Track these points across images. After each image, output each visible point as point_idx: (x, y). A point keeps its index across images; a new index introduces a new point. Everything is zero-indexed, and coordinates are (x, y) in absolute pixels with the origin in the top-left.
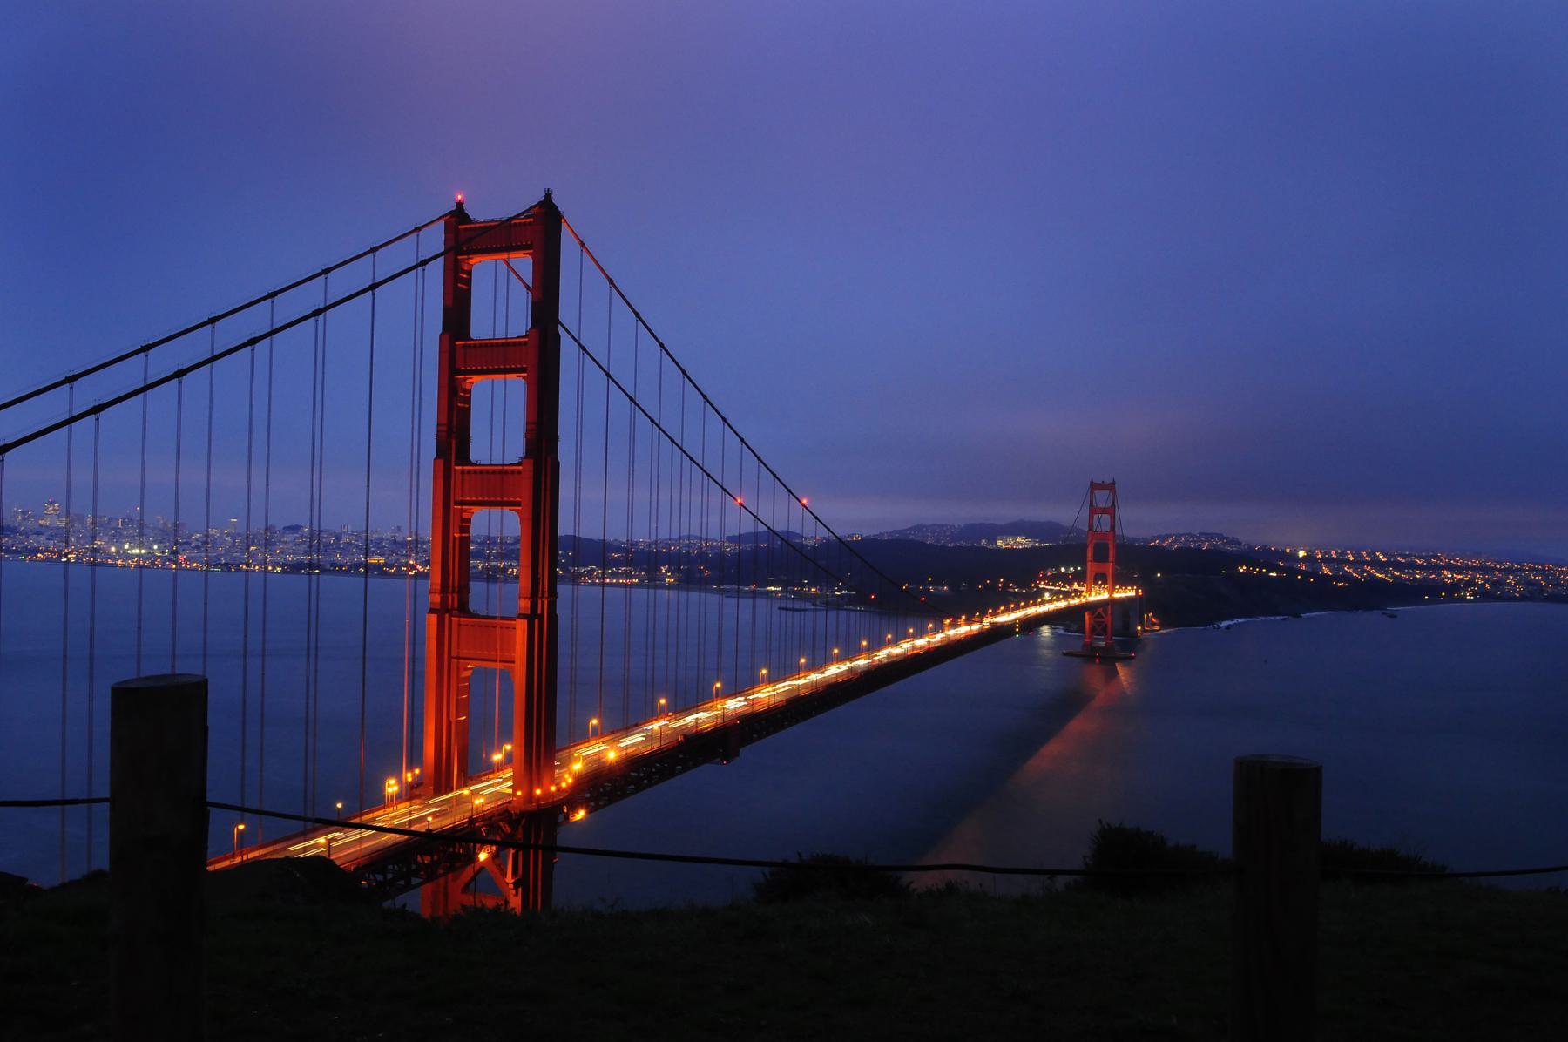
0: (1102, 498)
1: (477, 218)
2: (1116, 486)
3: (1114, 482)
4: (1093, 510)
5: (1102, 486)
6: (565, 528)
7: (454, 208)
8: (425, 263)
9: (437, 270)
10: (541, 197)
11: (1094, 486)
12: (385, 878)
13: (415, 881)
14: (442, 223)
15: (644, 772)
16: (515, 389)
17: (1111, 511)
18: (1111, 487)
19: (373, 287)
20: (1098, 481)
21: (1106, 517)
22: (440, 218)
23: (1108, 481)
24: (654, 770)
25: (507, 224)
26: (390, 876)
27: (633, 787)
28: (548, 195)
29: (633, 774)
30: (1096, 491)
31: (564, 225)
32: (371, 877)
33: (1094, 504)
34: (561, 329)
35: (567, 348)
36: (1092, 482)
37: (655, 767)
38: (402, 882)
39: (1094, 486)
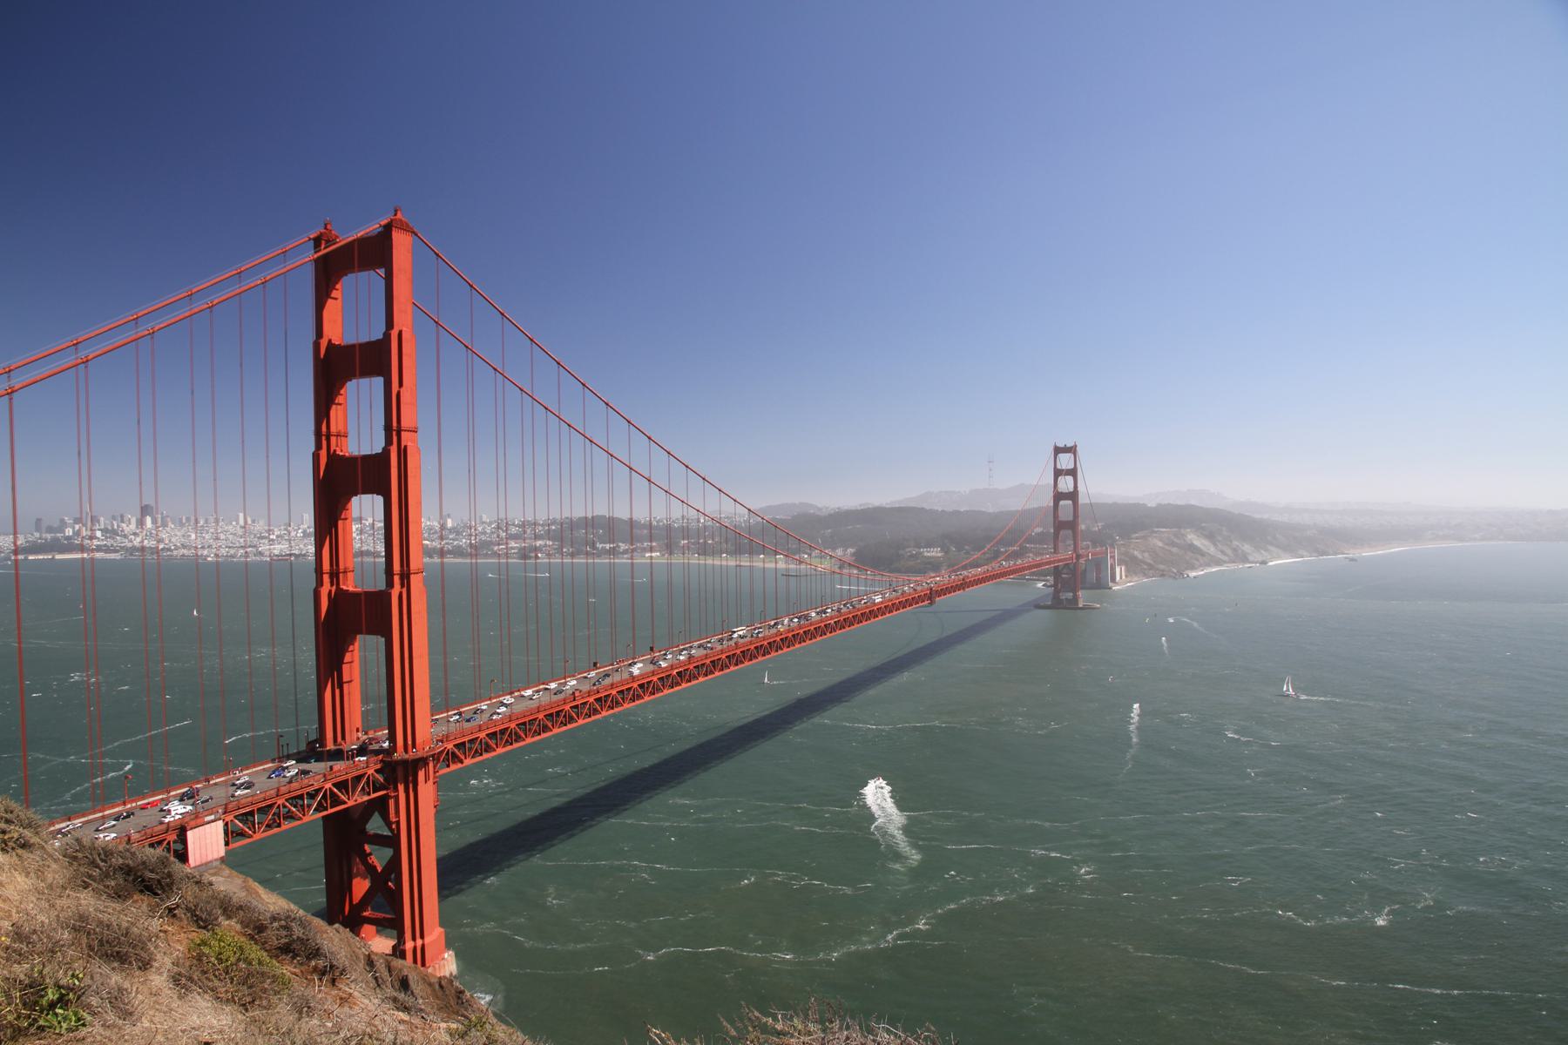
0: (1065, 461)
2: (1078, 448)
3: (1076, 446)
4: (1058, 473)
5: (1066, 450)
14: (312, 242)
17: (1073, 473)
18: (1072, 450)
20: (1063, 446)
21: (1070, 479)
22: (310, 239)
23: (1068, 445)
25: (362, 241)
30: (1060, 455)
33: (1059, 467)
39: (1058, 450)
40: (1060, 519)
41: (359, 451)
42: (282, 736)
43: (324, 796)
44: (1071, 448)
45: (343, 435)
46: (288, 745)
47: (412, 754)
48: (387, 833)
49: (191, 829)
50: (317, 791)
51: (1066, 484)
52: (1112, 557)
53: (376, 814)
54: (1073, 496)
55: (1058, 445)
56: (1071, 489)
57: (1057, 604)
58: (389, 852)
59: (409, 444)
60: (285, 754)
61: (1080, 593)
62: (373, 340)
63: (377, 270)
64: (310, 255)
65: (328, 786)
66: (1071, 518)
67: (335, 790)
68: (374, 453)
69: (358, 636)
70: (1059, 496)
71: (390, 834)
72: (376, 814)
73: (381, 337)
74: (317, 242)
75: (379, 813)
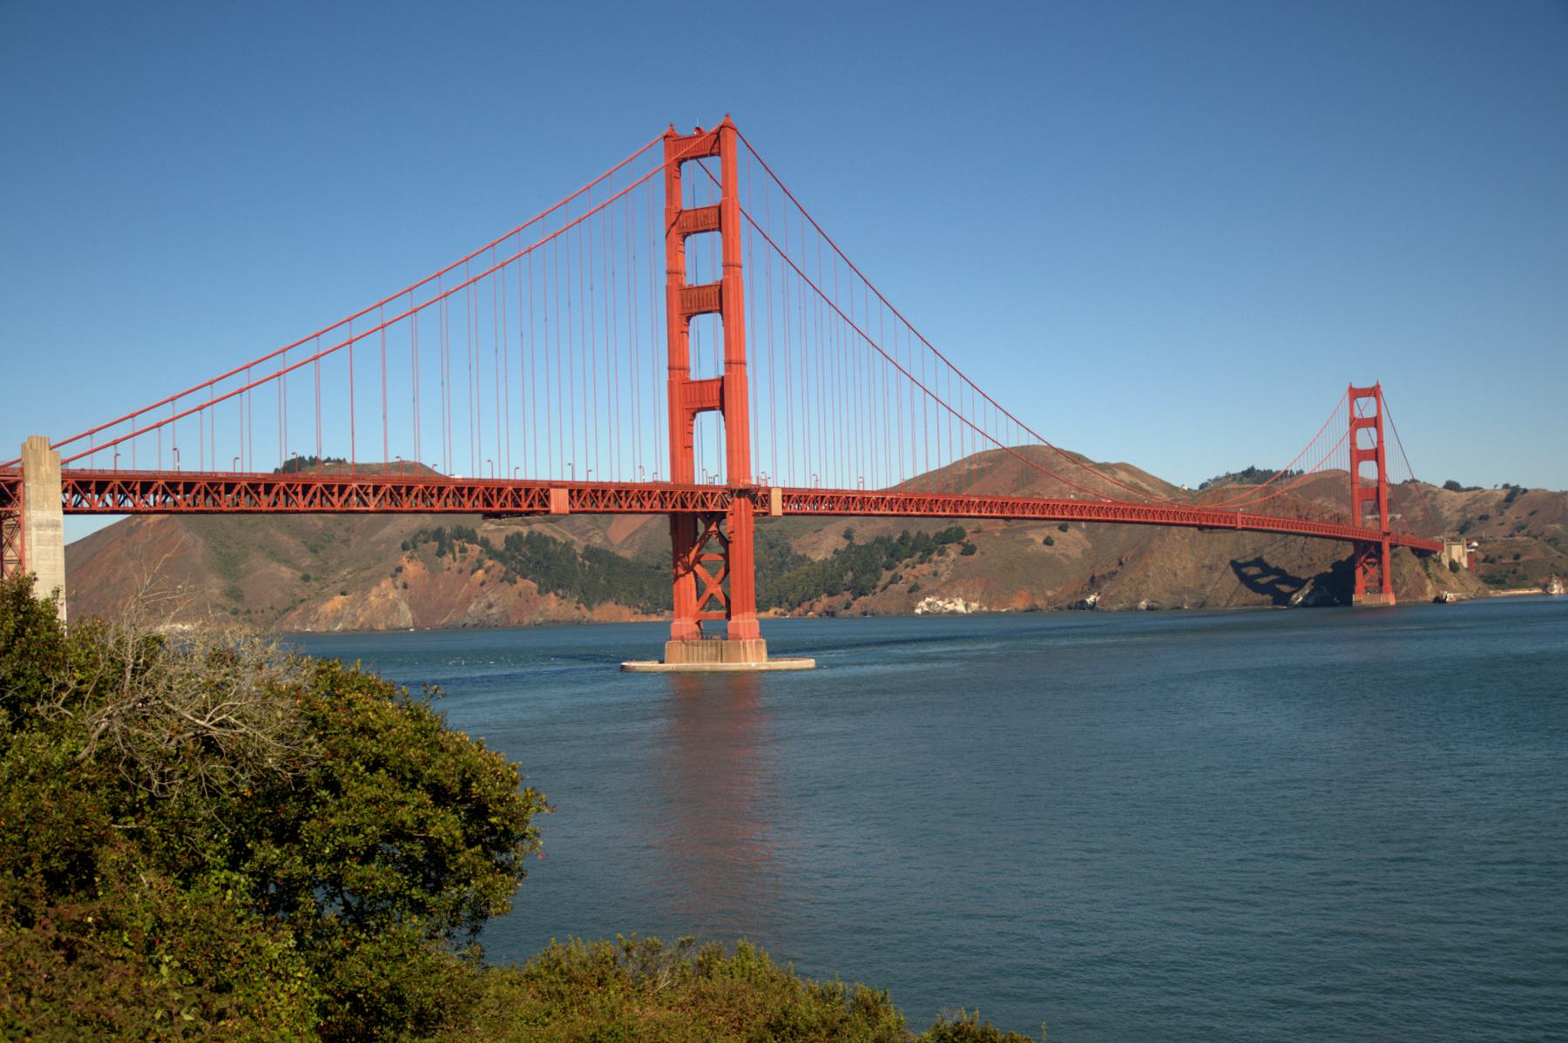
0: (1367, 408)
2: (1382, 389)
3: (1378, 386)
4: (1356, 424)
17: (1376, 422)
18: (1374, 392)
23: (1371, 384)
30: (1359, 399)
36: (1351, 389)
39: (1355, 393)
44: (1373, 388)
51: (1366, 440)
54: (1377, 455)
55: (1354, 386)
63: (700, 160)
70: (1358, 456)
74: (665, 137)
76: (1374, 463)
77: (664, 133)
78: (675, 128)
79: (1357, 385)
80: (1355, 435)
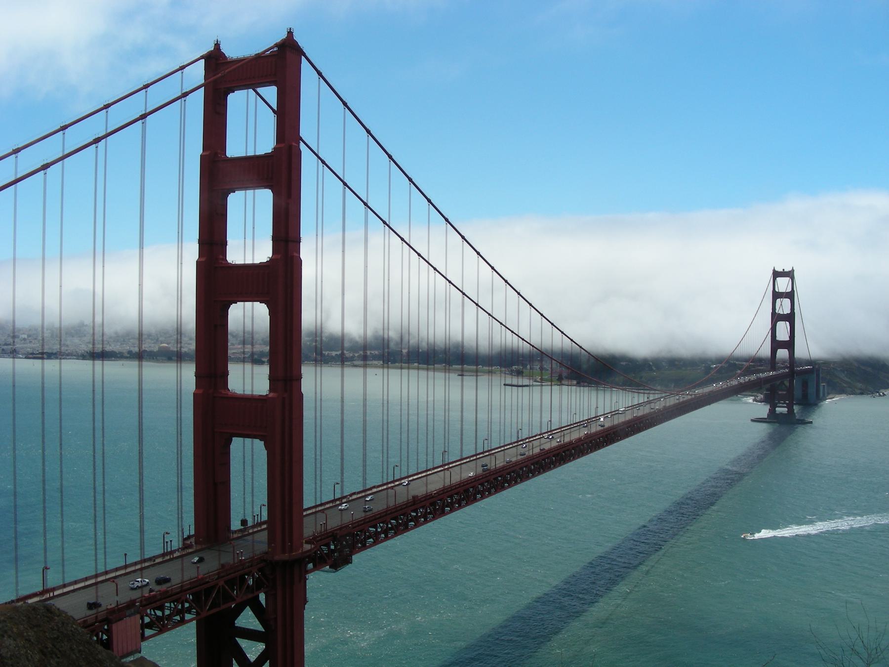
0: (783, 284)
1: (231, 56)
3: (793, 270)
4: (776, 295)
5: (783, 274)
6: (308, 317)
7: (213, 49)
8: (185, 95)
9: (197, 100)
10: (284, 35)
11: (776, 274)
12: (163, 614)
13: (188, 617)
14: (203, 61)
15: (381, 527)
16: (264, 198)
17: (790, 295)
18: (790, 274)
19: (143, 117)
20: (779, 269)
21: (787, 302)
22: (202, 57)
23: (785, 270)
24: (390, 526)
26: (167, 612)
27: (371, 540)
28: (290, 33)
29: (371, 529)
30: (779, 279)
31: (303, 58)
32: (153, 613)
33: (777, 290)
34: (302, 146)
35: (308, 164)
37: (391, 523)
38: (178, 618)
39: (776, 274)
40: (777, 339)
41: (253, 260)
42: (167, 533)
43: (218, 591)
44: (790, 272)
45: (224, 244)
46: (171, 541)
47: (286, 557)
48: (260, 628)
49: (116, 622)
50: (213, 587)
51: (784, 306)
52: (818, 375)
53: (248, 608)
55: (776, 269)
56: (787, 311)
57: (773, 418)
58: (261, 647)
59: (295, 254)
60: (169, 550)
61: (796, 408)
62: (258, 153)
64: (197, 73)
65: (221, 583)
66: (787, 339)
67: (227, 587)
68: (257, 261)
69: (233, 438)
71: (260, 628)
72: (248, 608)
73: (270, 151)
75: (250, 607)
76: (788, 323)
77: (204, 52)
78: (222, 47)
79: (779, 269)
80: (775, 303)
